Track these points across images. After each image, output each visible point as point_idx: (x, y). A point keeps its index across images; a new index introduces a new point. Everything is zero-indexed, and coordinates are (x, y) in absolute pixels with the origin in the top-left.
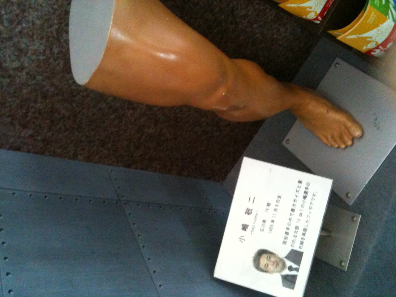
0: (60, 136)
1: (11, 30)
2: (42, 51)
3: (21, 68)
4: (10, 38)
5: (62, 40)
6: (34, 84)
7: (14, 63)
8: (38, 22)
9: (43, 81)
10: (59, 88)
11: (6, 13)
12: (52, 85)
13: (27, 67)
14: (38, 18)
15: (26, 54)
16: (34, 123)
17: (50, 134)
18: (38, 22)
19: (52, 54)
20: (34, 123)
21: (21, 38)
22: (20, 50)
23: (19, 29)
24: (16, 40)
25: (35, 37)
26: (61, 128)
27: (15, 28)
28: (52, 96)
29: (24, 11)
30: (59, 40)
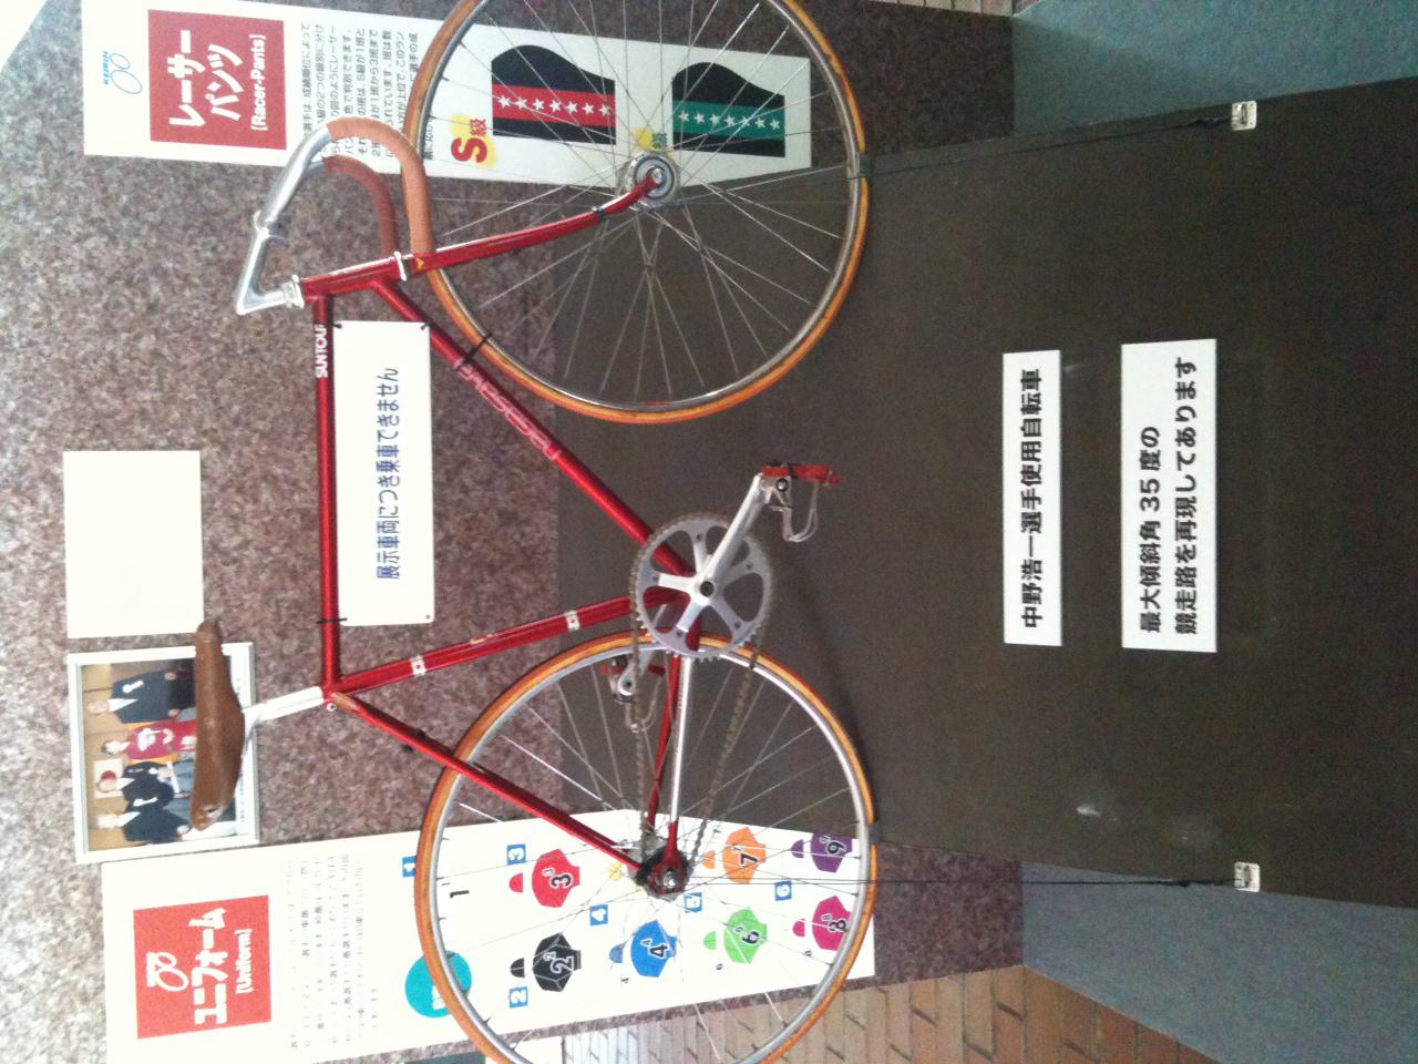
0: (90, 346)
1: (114, 293)
2: (61, 275)
3: (246, 544)
4: (111, 281)
5: (38, 299)
6: (167, 430)
7: (93, 245)
8: (82, 316)
9: (40, 227)
10: (127, 435)
11: (126, 314)
12: (23, 223)
13: (73, 243)
14: (83, 322)
15: (82, 262)
16: (397, 814)
17: (110, 346)
18: (82, 316)
19: (44, 275)
20: (397, 814)
21: (97, 287)
22: (91, 267)
23: (105, 297)
24: (103, 281)
25: (78, 291)
26: (95, 362)
27: (109, 299)
28: (132, 417)
29: (106, 325)
30: (42, 298)
